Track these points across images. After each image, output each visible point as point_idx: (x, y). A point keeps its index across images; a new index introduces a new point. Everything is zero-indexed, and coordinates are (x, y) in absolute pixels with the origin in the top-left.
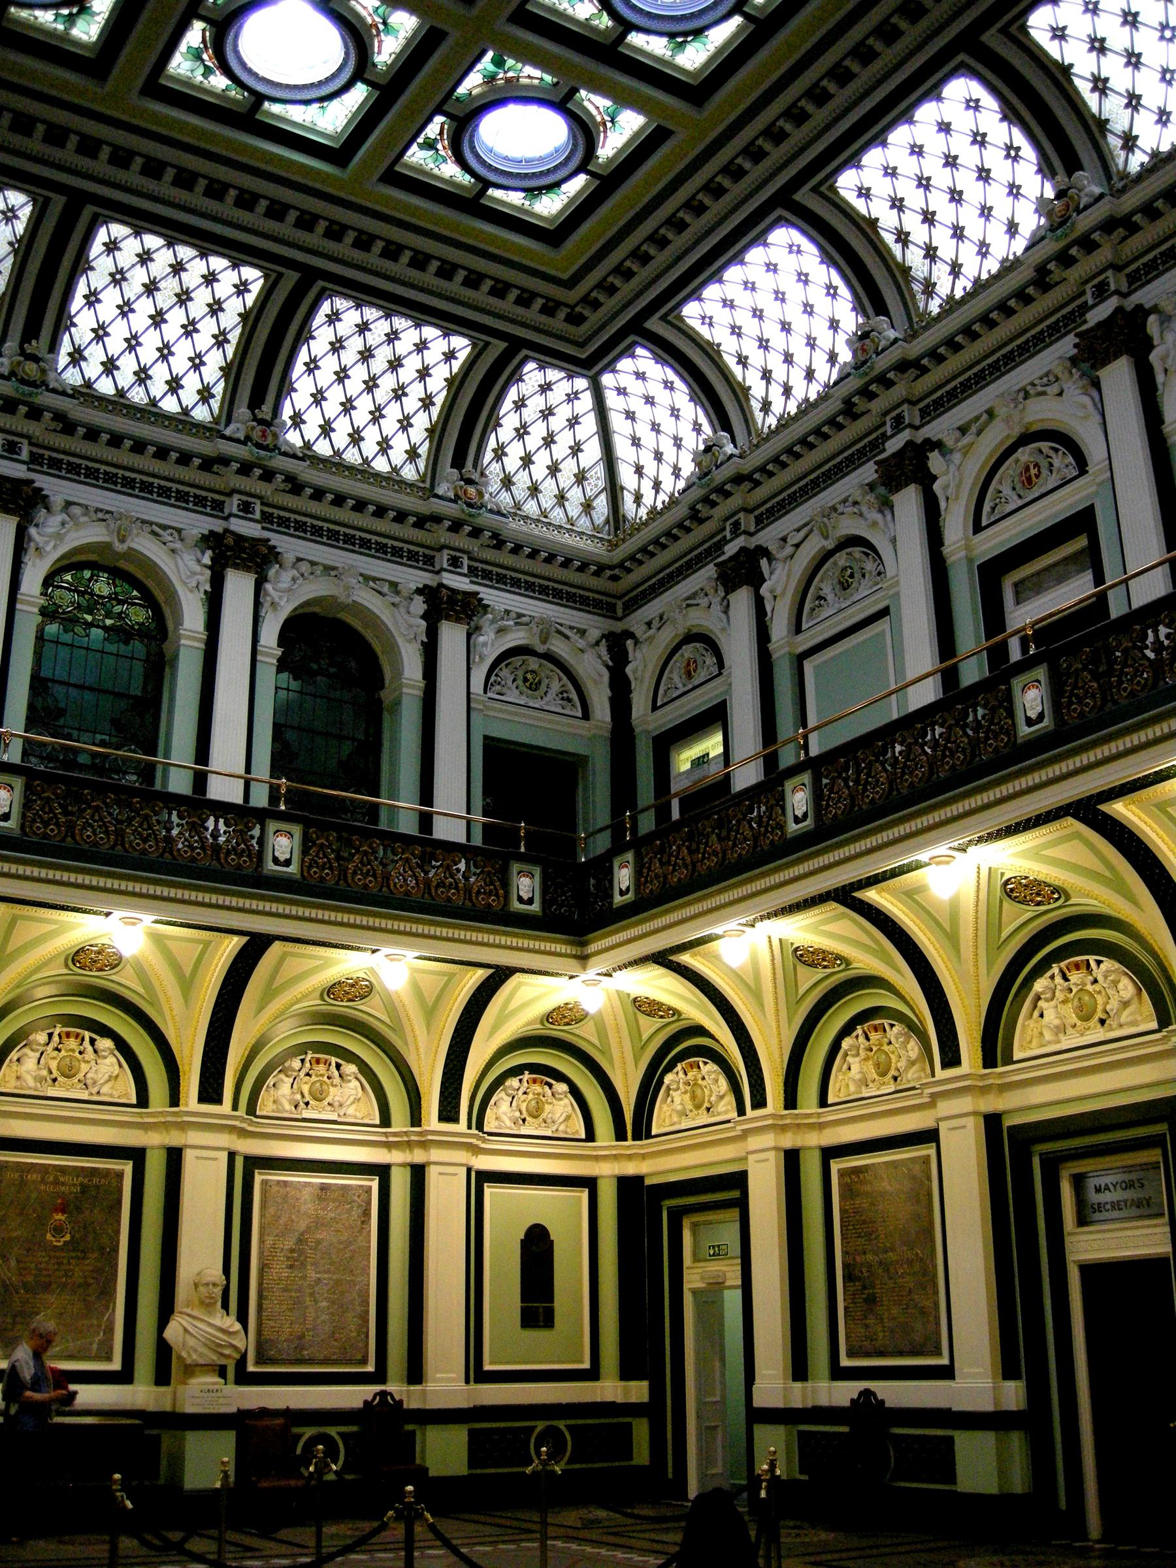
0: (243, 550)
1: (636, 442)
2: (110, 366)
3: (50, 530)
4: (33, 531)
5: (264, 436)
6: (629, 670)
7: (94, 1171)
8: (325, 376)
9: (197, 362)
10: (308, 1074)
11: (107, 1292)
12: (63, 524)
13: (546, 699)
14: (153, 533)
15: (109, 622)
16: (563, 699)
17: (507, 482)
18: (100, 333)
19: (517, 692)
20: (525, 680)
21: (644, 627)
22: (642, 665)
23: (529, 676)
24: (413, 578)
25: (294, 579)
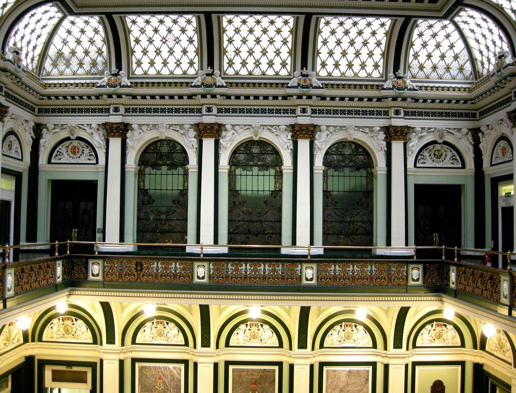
0: (303, 130)
2: (244, 64)
3: (229, 138)
4: (221, 141)
5: (305, 82)
6: (481, 146)
7: (265, 370)
8: (332, 44)
9: (278, 53)
10: (344, 330)
12: (233, 134)
13: (444, 161)
14: (268, 129)
15: (259, 163)
16: (453, 159)
17: (421, 67)
18: (237, 52)
19: (431, 161)
20: (435, 155)
21: (486, 128)
22: (486, 145)
23: (436, 153)
24: (379, 123)
25: (328, 135)
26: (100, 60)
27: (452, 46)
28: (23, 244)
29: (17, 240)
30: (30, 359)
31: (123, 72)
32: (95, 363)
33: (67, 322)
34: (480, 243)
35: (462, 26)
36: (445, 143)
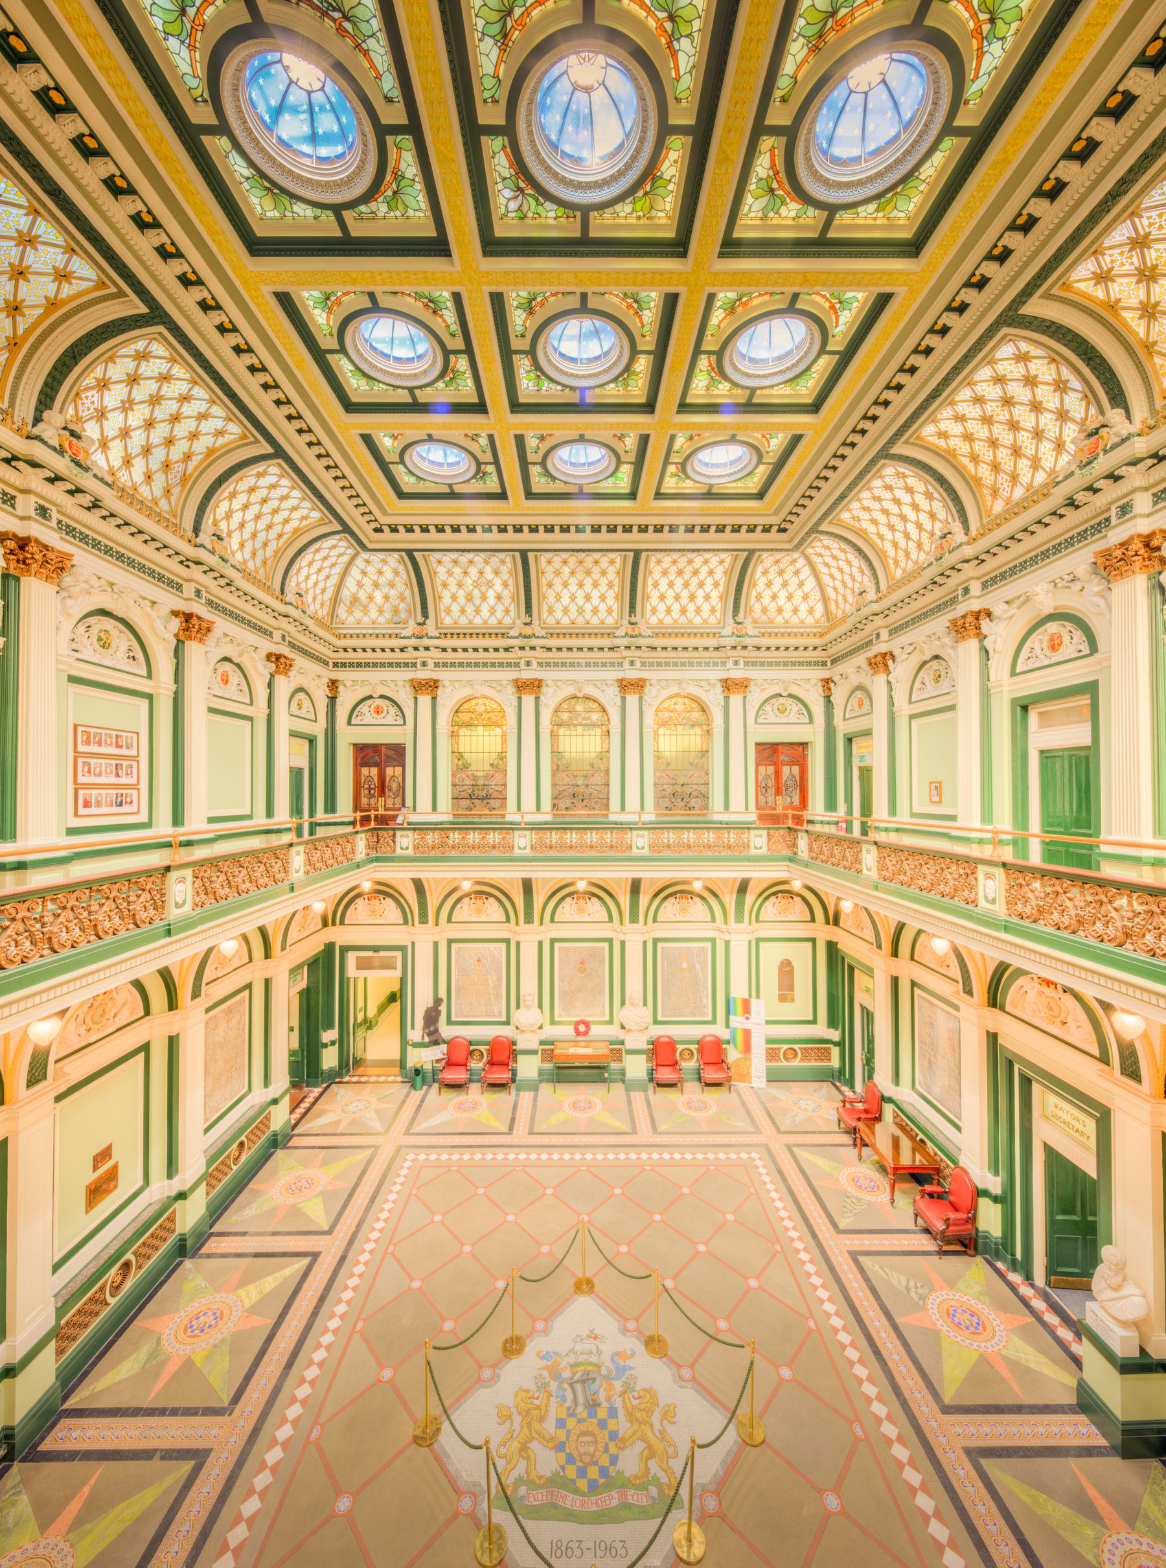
1: (832, 576)
2: (566, 611)
8: (663, 587)
11: (601, 992)
22: (838, 696)
26: (402, 606)
27: (801, 584)
28: (321, 815)
29: (312, 813)
30: (330, 947)
31: (430, 622)
32: (406, 947)
33: (374, 902)
34: (831, 805)
35: (815, 559)
36: (791, 696)
